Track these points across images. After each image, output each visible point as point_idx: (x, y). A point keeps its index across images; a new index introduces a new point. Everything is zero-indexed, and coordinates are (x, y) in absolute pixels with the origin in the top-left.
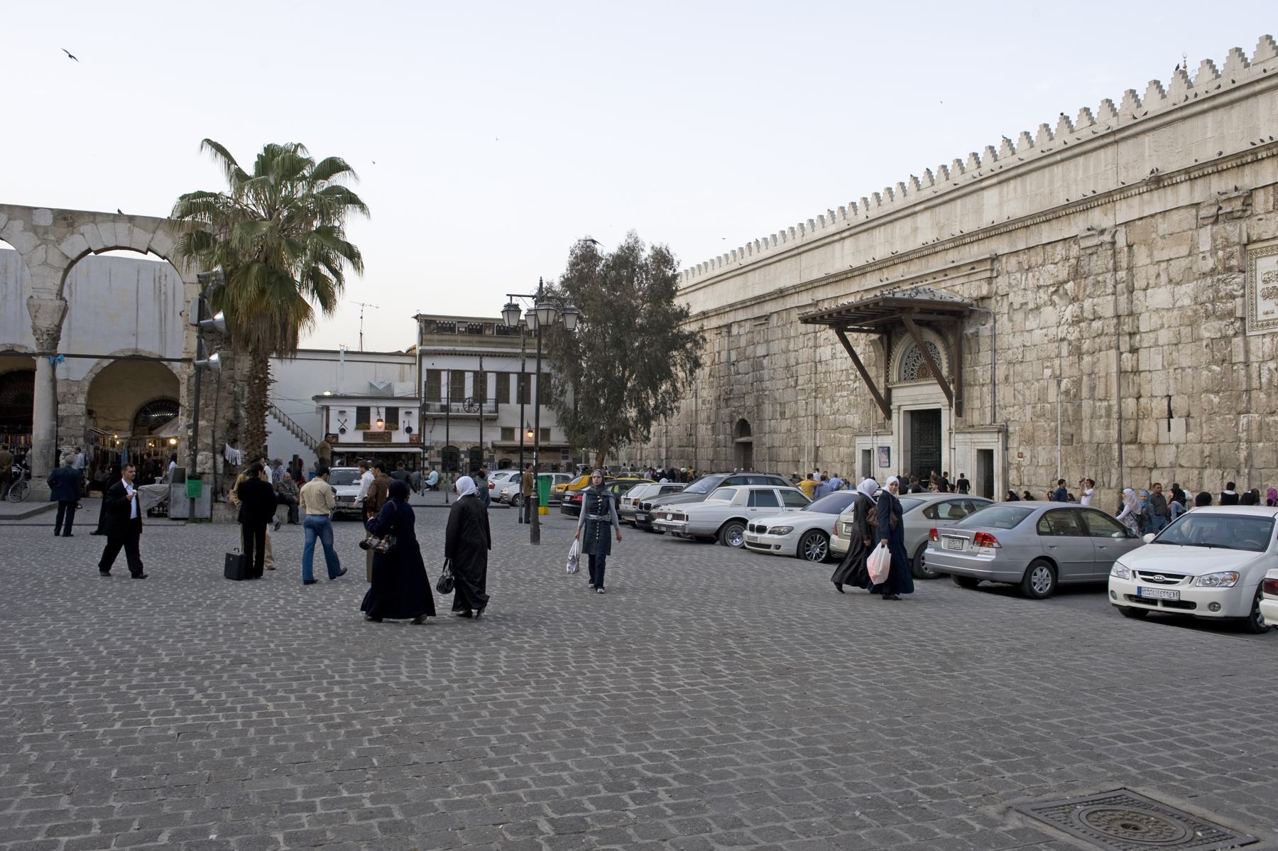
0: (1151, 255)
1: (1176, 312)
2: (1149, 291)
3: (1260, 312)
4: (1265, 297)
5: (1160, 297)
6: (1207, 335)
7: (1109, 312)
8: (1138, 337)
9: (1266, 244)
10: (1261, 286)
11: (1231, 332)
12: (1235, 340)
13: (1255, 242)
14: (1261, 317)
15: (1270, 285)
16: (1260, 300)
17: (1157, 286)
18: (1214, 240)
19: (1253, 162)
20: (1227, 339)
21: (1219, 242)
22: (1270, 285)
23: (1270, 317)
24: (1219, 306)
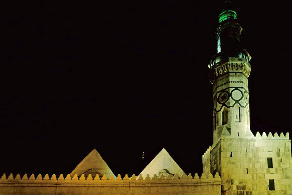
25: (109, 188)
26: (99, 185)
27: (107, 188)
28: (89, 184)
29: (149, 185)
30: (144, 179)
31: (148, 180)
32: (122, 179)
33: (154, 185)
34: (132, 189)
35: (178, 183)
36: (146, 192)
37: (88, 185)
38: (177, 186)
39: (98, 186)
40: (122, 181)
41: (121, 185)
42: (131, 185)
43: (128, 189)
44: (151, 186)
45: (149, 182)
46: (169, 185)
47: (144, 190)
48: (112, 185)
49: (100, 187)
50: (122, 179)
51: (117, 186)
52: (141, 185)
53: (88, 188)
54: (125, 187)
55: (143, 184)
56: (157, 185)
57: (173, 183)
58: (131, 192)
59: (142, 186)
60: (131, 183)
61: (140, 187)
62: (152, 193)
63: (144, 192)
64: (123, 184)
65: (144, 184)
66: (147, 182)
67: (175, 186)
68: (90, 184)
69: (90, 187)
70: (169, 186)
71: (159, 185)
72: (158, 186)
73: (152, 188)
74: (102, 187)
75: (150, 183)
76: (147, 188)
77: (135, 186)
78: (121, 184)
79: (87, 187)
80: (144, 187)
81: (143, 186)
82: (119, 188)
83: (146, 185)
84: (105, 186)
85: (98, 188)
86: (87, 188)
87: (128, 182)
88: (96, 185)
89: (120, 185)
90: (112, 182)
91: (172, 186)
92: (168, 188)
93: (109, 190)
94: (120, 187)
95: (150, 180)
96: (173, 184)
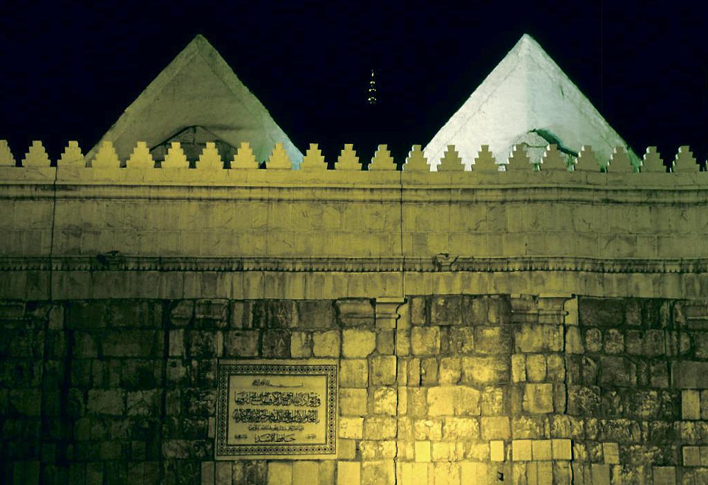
0: (99, 347)
1: (127, 423)
2: (92, 392)
3: (232, 434)
4: (237, 419)
5: (108, 400)
6: (171, 454)
7: (34, 408)
8: (71, 447)
9: (242, 362)
10: (233, 406)
11: (201, 454)
12: (205, 464)
13: (231, 358)
14: (232, 441)
15: (245, 407)
16: (232, 421)
17: (105, 386)
18: (188, 346)
19: (237, 270)
20: (198, 462)
21: (193, 349)
22: (245, 407)
23: (243, 442)
24: (189, 422)
25: (304, 206)
26: (256, 194)
27: (296, 205)
28: (207, 187)
29: (496, 196)
30: (468, 168)
31: (484, 173)
32: (365, 168)
33: (520, 196)
34: (411, 212)
35: (634, 191)
36: (482, 224)
37: (204, 190)
38: (627, 202)
39: (253, 196)
40: (363, 178)
41: (360, 196)
42: (407, 196)
43: (395, 212)
44: (503, 202)
45: (490, 183)
46: (587, 196)
47: (470, 217)
48: (318, 194)
49: (262, 200)
50: (365, 168)
51: (346, 197)
52: (458, 196)
53: (208, 207)
54: (381, 202)
55: (465, 190)
56: (531, 198)
57: (607, 191)
58: (410, 224)
59: (459, 198)
60: (409, 184)
61: (450, 202)
62: (510, 229)
63: (473, 226)
64: (372, 190)
65: (472, 191)
66: (481, 183)
67: (618, 203)
68: (217, 188)
69: (217, 203)
70: (591, 203)
71: (540, 195)
72: (535, 201)
73: (509, 211)
74: (269, 200)
75: (496, 187)
76: (484, 210)
77: (430, 202)
78: (359, 189)
79: (201, 199)
80: (469, 204)
81: (467, 197)
82: (350, 204)
83: (480, 196)
84: (285, 195)
85: (254, 205)
86: (203, 203)
87: (395, 182)
88: (246, 194)
89: (356, 192)
90: (315, 181)
91: (607, 201)
92: (585, 212)
93: (305, 215)
94: (358, 201)
95: (495, 172)
96: (611, 196)
